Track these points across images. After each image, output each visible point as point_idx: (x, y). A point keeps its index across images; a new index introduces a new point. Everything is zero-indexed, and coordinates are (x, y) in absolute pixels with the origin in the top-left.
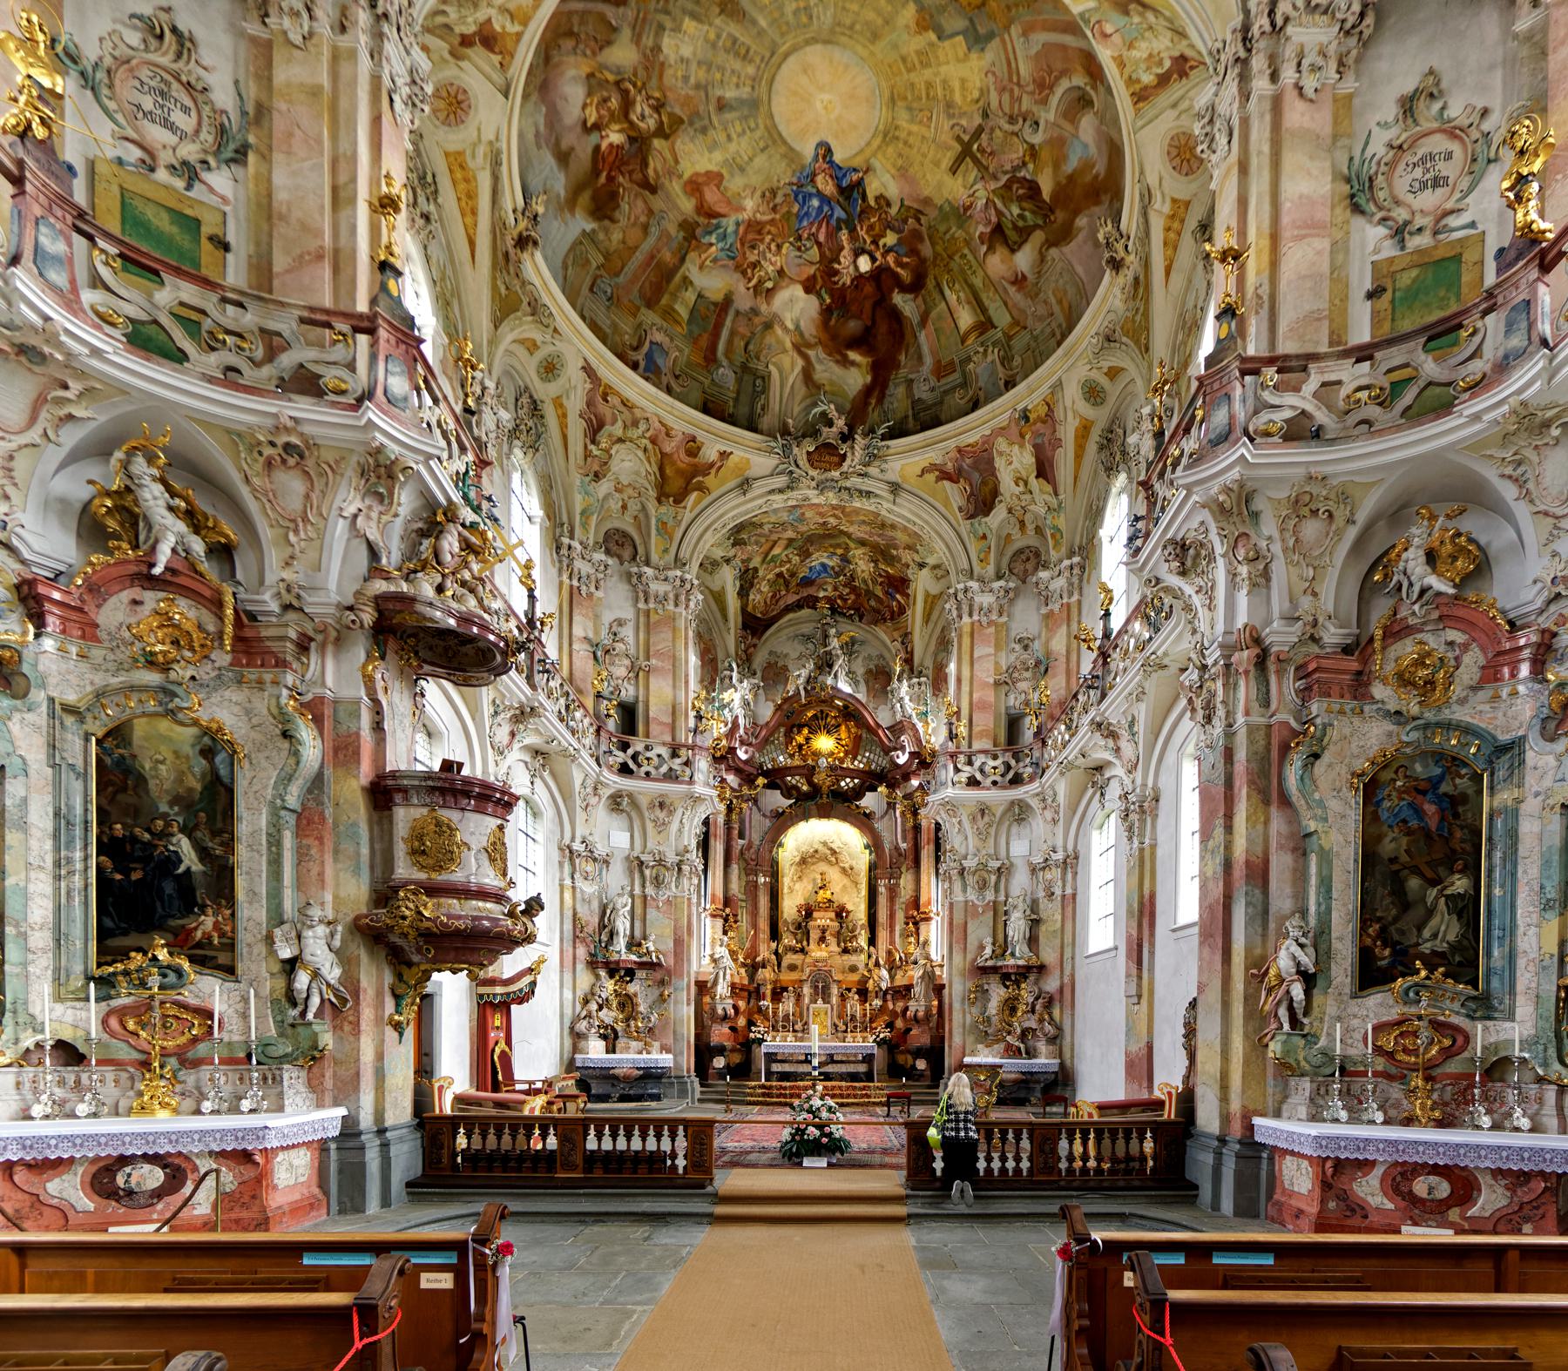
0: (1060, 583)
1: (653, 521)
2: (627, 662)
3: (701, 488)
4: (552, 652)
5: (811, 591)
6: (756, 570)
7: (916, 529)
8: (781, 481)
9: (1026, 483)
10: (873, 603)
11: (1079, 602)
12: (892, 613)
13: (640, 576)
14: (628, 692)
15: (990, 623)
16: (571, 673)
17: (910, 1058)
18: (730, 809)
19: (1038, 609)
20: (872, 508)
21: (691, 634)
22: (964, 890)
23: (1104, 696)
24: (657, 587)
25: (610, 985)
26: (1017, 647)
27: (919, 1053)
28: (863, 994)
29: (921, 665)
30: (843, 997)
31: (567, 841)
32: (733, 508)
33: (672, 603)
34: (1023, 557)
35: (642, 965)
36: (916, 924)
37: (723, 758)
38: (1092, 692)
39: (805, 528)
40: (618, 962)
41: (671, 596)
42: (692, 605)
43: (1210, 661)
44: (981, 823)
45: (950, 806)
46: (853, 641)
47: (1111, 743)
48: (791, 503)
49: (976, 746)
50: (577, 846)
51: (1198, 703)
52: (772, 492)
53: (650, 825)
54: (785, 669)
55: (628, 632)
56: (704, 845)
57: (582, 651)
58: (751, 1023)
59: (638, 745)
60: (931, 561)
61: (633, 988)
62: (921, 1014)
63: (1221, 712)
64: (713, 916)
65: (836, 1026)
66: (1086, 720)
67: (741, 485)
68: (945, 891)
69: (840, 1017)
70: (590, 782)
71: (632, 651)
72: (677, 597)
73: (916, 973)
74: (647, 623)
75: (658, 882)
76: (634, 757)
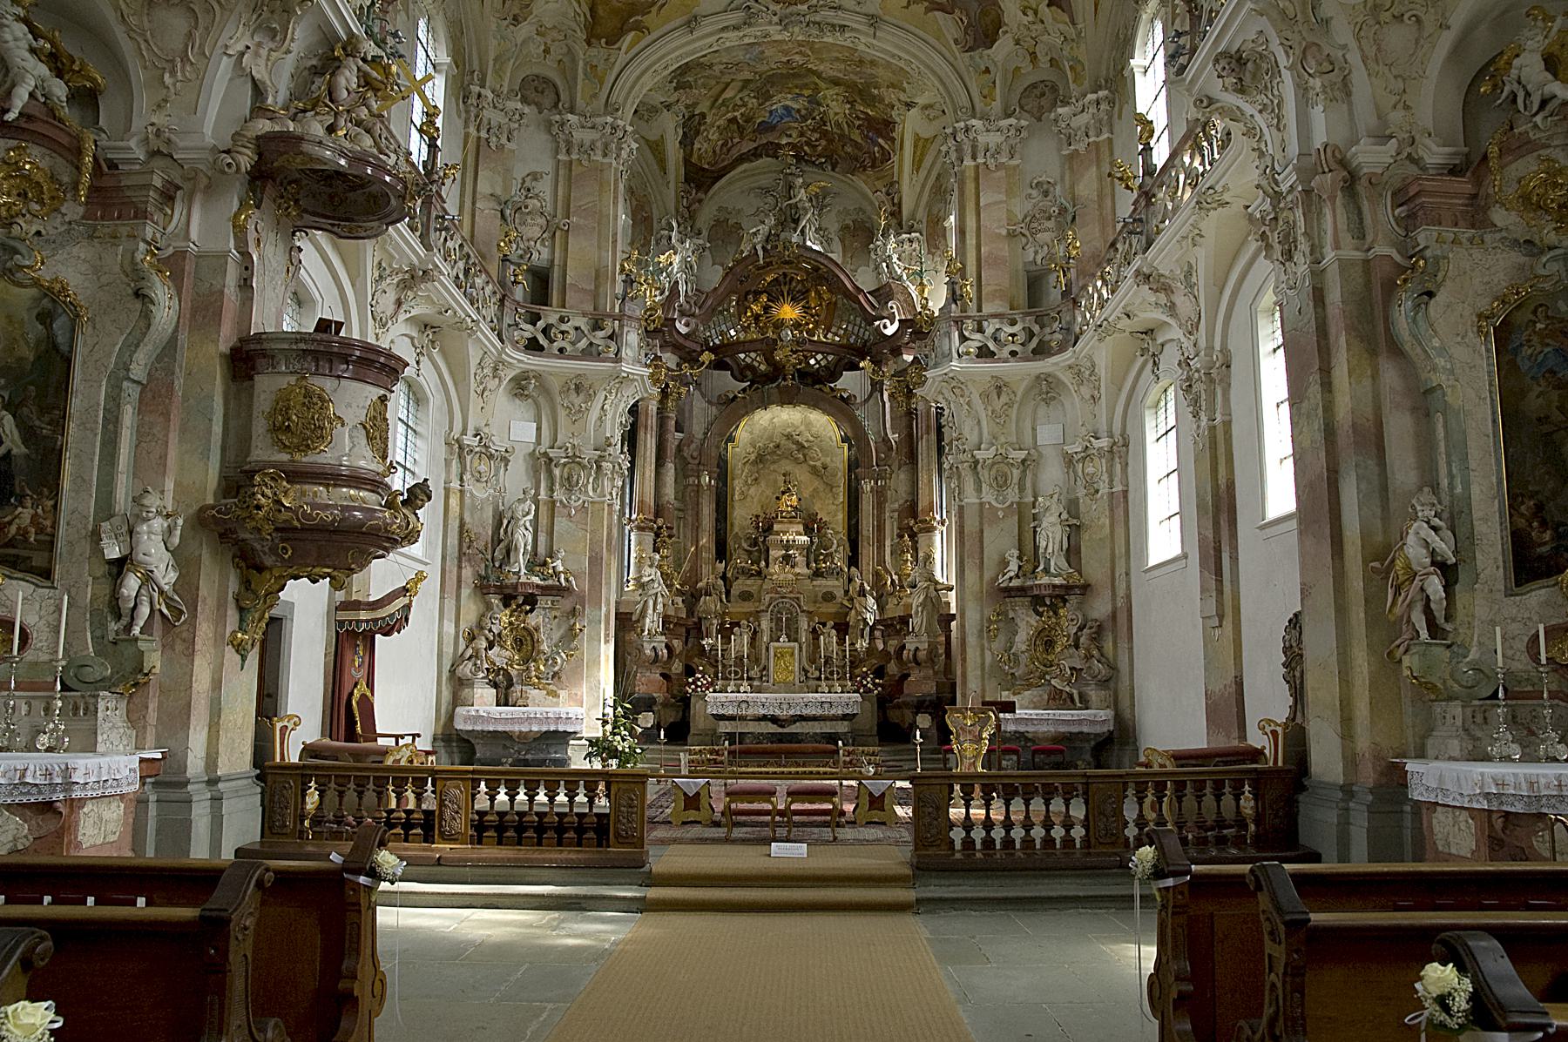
0: (1084, 119)
1: (581, 64)
2: (542, 221)
3: (640, 28)
4: (452, 208)
5: (771, 137)
6: (703, 116)
7: (902, 64)
8: (735, 17)
9: (1036, 13)
10: (849, 149)
11: (1110, 140)
12: (874, 160)
13: (562, 125)
14: (541, 255)
15: (998, 167)
16: (472, 236)
17: (908, 713)
18: (665, 393)
19: (1059, 150)
20: (848, 43)
21: (621, 186)
22: (979, 490)
23: (1149, 244)
24: (582, 136)
25: (504, 617)
26: (1034, 193)
27: (920, 706)
28: (842, 629)
29: (913, 217)
30: (815, 633)
31: (456, 434)
32: (678, 48)
33: (599, 152)
34: (1037, 92)
35: (546, 590)
36: (913, 536)
37: (658, 332)
38: (1134, 239)
39: (765, 68)
40: (515, 586)
41: (599, 144)
42: (624, 154)
43: (1284, 188)
44: (998, 404)
45: (956, 384)
46: (825, 193)
47: (1162, 298)
48: (746, 40)
49: (987, 309)
50: (470, 440)
51: (1274, 238)
52: (724, 29)
53: (562, 413)
54: (739, 226)
55: (544, 187)
56: (631, 439)
57: (486, 208)
58: (690, 671)
59: (550, 316)
60: (921, 100)
61: (533, 620)
62: (922, 655)
63: (1303, 245)
64: (640, 528)
65: (806, 672)
66: (1129, 272)
67: (689, 22)
68: (951, 492)
69: (812, 661)
70: (489, 361)
71: (549, 208)
72: (606, 146)
73: (916, 600)
74: (568, 174)
75: (570, 484)
76: (545, 331)
